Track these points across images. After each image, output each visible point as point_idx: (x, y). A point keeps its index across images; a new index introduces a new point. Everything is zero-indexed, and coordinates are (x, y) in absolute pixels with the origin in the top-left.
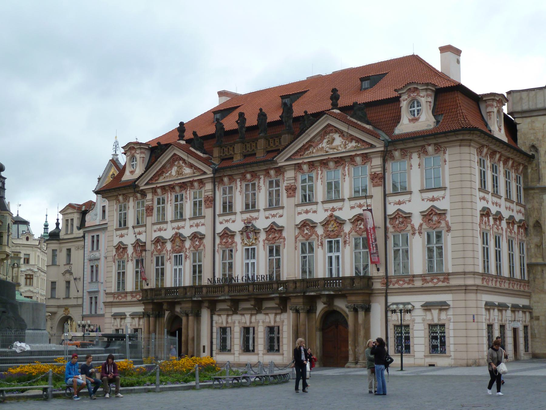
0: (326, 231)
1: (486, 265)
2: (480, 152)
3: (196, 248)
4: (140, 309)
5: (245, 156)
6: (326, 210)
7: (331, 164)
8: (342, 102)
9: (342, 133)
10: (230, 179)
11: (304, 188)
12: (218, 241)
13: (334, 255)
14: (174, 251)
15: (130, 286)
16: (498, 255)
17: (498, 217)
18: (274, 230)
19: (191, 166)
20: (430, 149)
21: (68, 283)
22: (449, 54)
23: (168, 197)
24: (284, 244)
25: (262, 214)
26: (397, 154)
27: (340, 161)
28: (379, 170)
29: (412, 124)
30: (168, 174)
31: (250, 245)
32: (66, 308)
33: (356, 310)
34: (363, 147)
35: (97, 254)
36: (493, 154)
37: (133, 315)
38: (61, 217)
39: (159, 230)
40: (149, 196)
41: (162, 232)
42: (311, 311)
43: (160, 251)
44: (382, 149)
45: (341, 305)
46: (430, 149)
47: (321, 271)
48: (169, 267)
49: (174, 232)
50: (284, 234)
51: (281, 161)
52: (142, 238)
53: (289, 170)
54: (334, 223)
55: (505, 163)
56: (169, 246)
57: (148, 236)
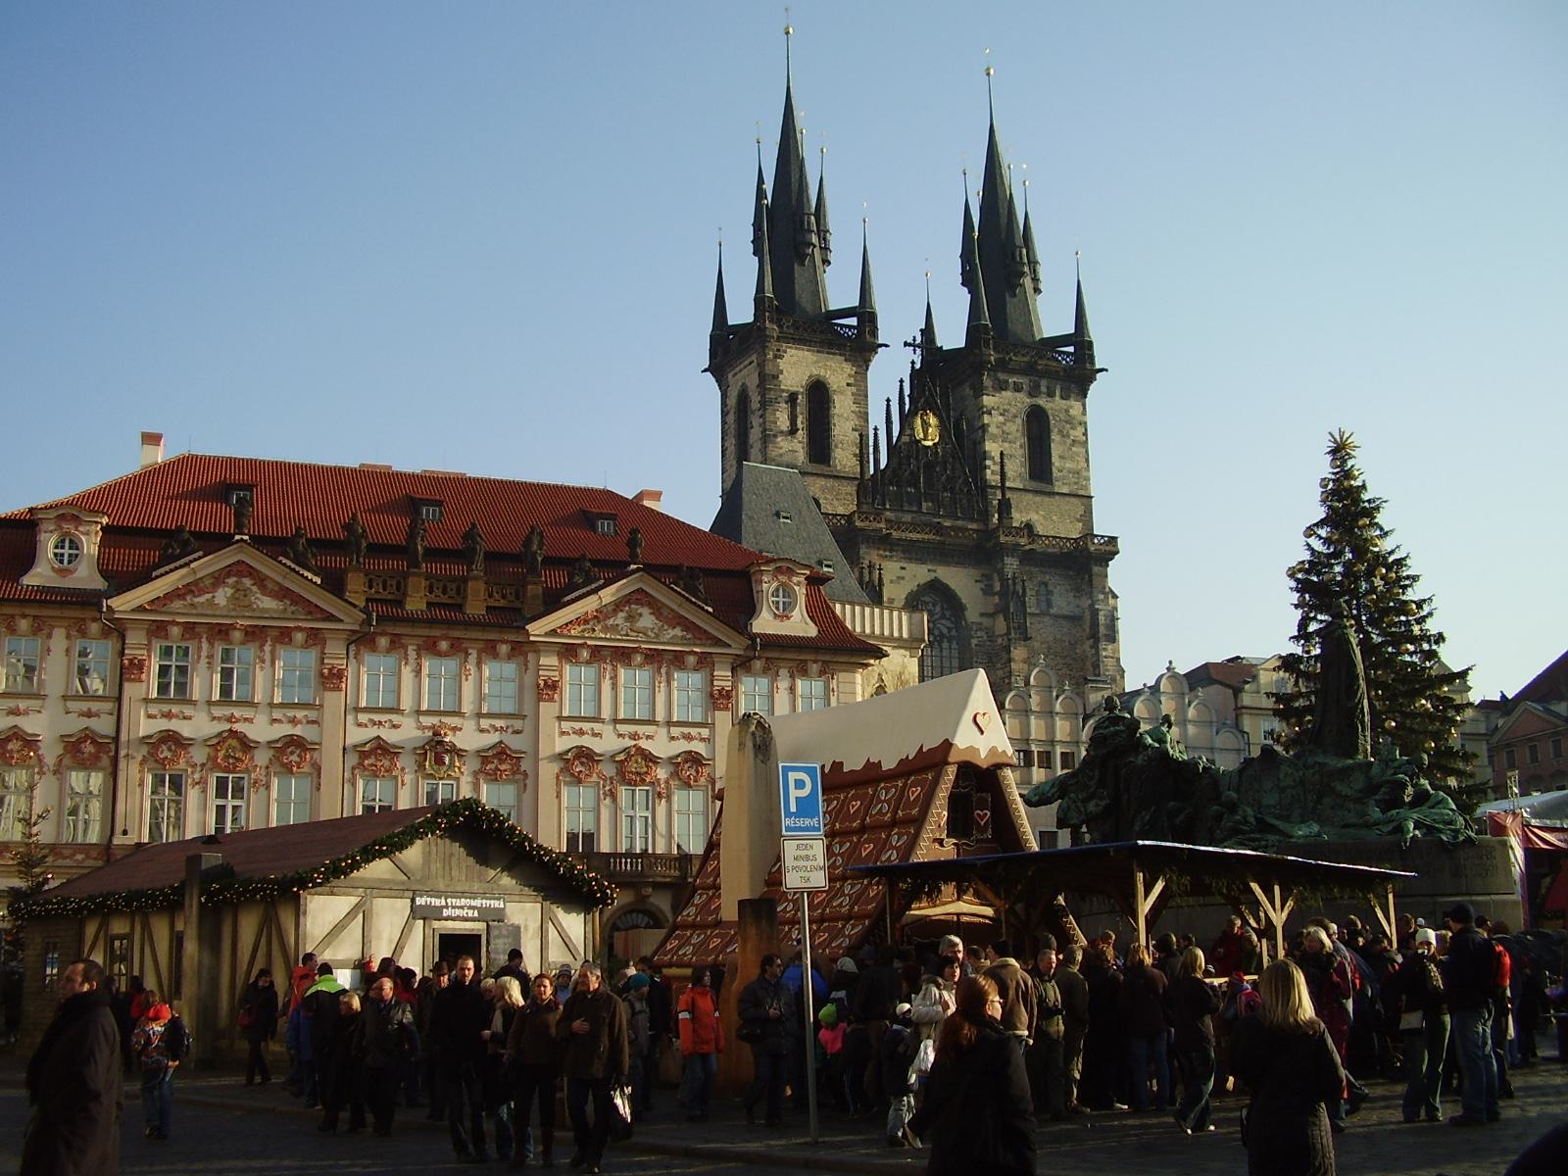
5: (429, 604)
6: (620, 735)
7: (639, 659)
9: (657, 609)
10: (392, 642)
19: (283, 593)
23: (200, 649)
24: (525, 785)
26: (758, 664)
27: (653, 657)
29: (777, 622)
30: (202, 599)
31: (441, 779)
34: (699, 642)
39: (164, 716)
40: (135, 638)
41: (174, 720)
44: (742, 653)
46: (815, 668)
49: (227, 726)
51: (537, 629)
53: (546, 651)
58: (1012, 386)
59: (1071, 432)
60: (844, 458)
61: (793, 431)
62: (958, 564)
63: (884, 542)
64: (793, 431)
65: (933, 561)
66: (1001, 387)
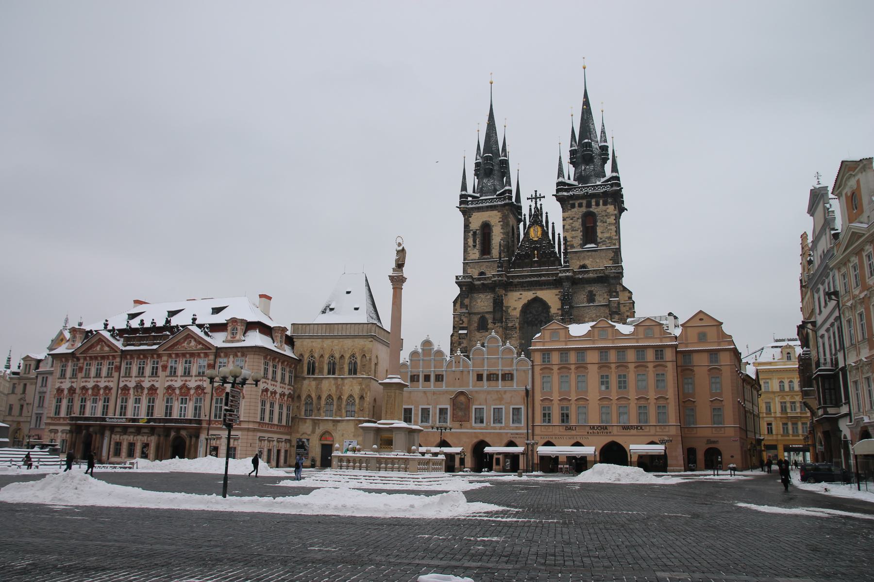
0: (181, 392)
1: (262, 418)
2: (265, 358)
3: (107, 394)
4: (68, 428)
8: (197, 322)
9: (195, 340)
11: (171, 367)
12: (120, 391)
13: (183, 406)
14: (93, 395)
15: (63, 414)
16: (271, 412)
17: (274, 393)
18: (153, 389)
20: (239, 354)
21: (22, 406)
22: (264, 299)
25: (147, 379)
26: (222, 354)
27: (192, 355)
28: (212, 362)
32: (19, 423)
33: (191, 437)
35: (45, 389)
36: (274, 360)
37: (63, 431)
38: (22, 362)
40: (82, 361)
42: (167, 436)
43: (84, 394)
45: (183, 433)
46: (239, 354)
47: (175, 415)
48: (89, 404)
50: (158, 392)
52: (74, 385)
54: (185, 389)
55: (282, 363)
56: (90, 392)
57: (78, 384)
58: (577, 205)
59: (608, 221)
60: (495, 252)
61: (475, 246)
62: (549, 289)
63: (509, 286)
64: (475, 246)
65: (535, 290)
66: (573, 206)
